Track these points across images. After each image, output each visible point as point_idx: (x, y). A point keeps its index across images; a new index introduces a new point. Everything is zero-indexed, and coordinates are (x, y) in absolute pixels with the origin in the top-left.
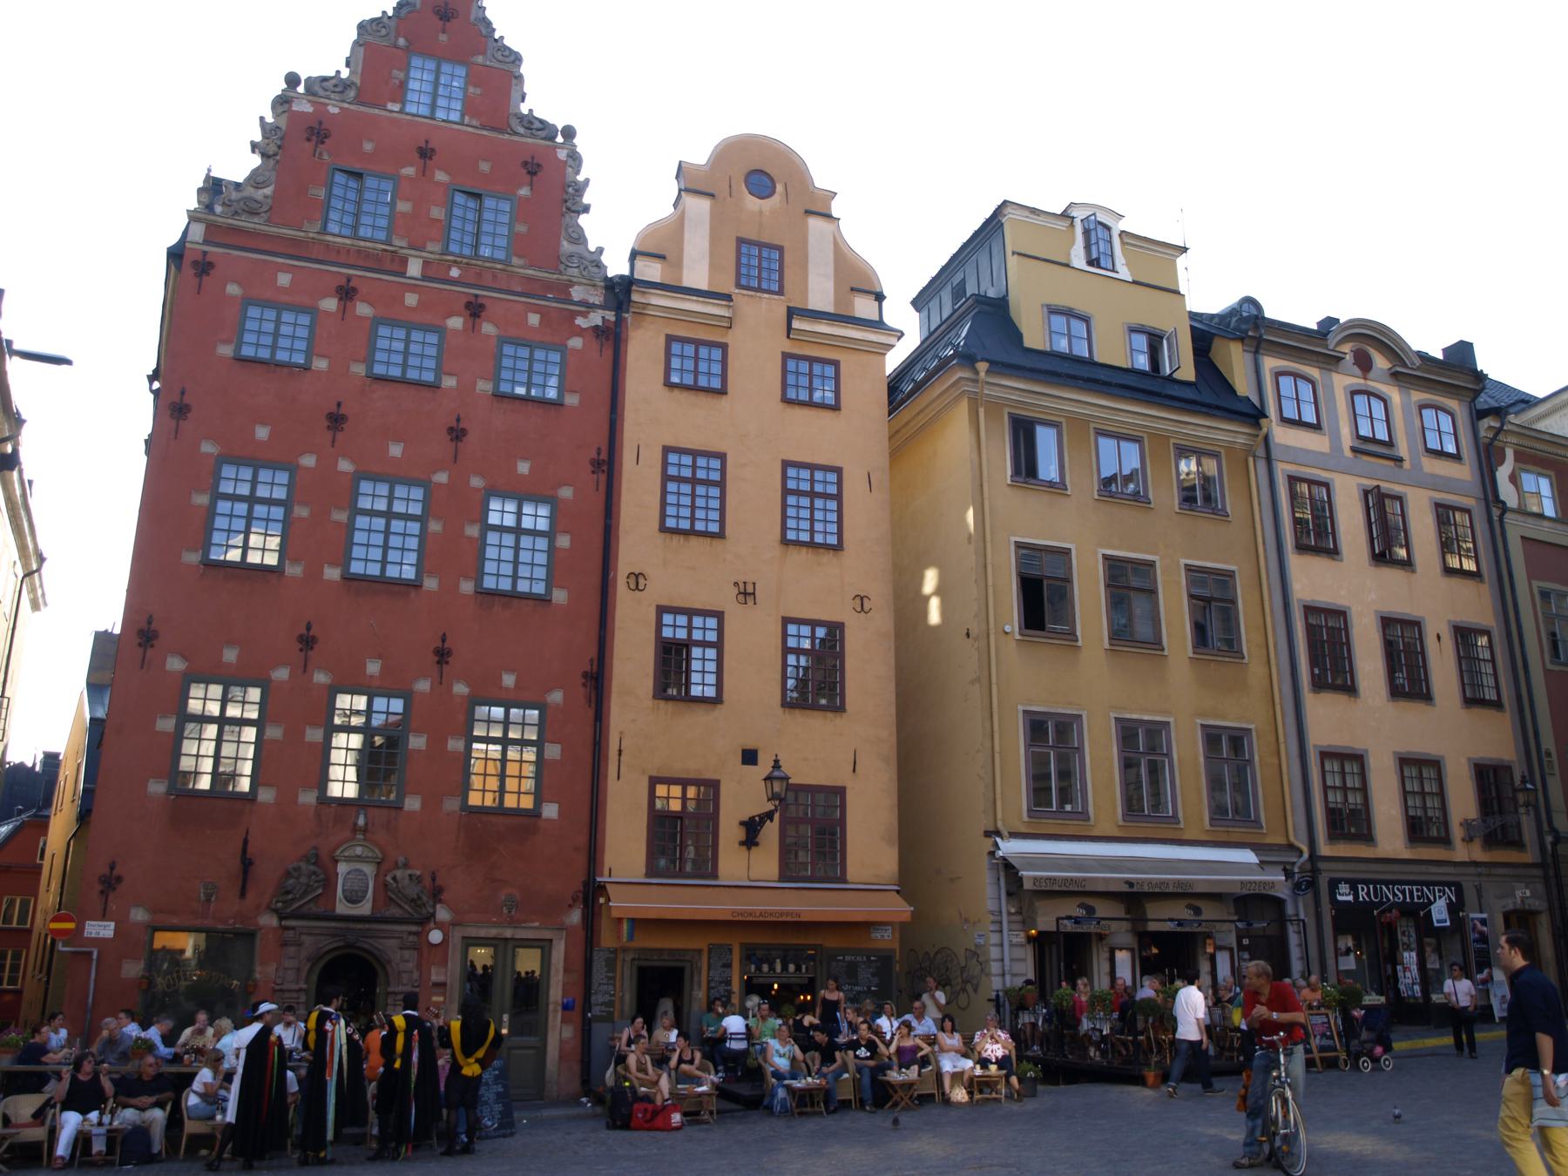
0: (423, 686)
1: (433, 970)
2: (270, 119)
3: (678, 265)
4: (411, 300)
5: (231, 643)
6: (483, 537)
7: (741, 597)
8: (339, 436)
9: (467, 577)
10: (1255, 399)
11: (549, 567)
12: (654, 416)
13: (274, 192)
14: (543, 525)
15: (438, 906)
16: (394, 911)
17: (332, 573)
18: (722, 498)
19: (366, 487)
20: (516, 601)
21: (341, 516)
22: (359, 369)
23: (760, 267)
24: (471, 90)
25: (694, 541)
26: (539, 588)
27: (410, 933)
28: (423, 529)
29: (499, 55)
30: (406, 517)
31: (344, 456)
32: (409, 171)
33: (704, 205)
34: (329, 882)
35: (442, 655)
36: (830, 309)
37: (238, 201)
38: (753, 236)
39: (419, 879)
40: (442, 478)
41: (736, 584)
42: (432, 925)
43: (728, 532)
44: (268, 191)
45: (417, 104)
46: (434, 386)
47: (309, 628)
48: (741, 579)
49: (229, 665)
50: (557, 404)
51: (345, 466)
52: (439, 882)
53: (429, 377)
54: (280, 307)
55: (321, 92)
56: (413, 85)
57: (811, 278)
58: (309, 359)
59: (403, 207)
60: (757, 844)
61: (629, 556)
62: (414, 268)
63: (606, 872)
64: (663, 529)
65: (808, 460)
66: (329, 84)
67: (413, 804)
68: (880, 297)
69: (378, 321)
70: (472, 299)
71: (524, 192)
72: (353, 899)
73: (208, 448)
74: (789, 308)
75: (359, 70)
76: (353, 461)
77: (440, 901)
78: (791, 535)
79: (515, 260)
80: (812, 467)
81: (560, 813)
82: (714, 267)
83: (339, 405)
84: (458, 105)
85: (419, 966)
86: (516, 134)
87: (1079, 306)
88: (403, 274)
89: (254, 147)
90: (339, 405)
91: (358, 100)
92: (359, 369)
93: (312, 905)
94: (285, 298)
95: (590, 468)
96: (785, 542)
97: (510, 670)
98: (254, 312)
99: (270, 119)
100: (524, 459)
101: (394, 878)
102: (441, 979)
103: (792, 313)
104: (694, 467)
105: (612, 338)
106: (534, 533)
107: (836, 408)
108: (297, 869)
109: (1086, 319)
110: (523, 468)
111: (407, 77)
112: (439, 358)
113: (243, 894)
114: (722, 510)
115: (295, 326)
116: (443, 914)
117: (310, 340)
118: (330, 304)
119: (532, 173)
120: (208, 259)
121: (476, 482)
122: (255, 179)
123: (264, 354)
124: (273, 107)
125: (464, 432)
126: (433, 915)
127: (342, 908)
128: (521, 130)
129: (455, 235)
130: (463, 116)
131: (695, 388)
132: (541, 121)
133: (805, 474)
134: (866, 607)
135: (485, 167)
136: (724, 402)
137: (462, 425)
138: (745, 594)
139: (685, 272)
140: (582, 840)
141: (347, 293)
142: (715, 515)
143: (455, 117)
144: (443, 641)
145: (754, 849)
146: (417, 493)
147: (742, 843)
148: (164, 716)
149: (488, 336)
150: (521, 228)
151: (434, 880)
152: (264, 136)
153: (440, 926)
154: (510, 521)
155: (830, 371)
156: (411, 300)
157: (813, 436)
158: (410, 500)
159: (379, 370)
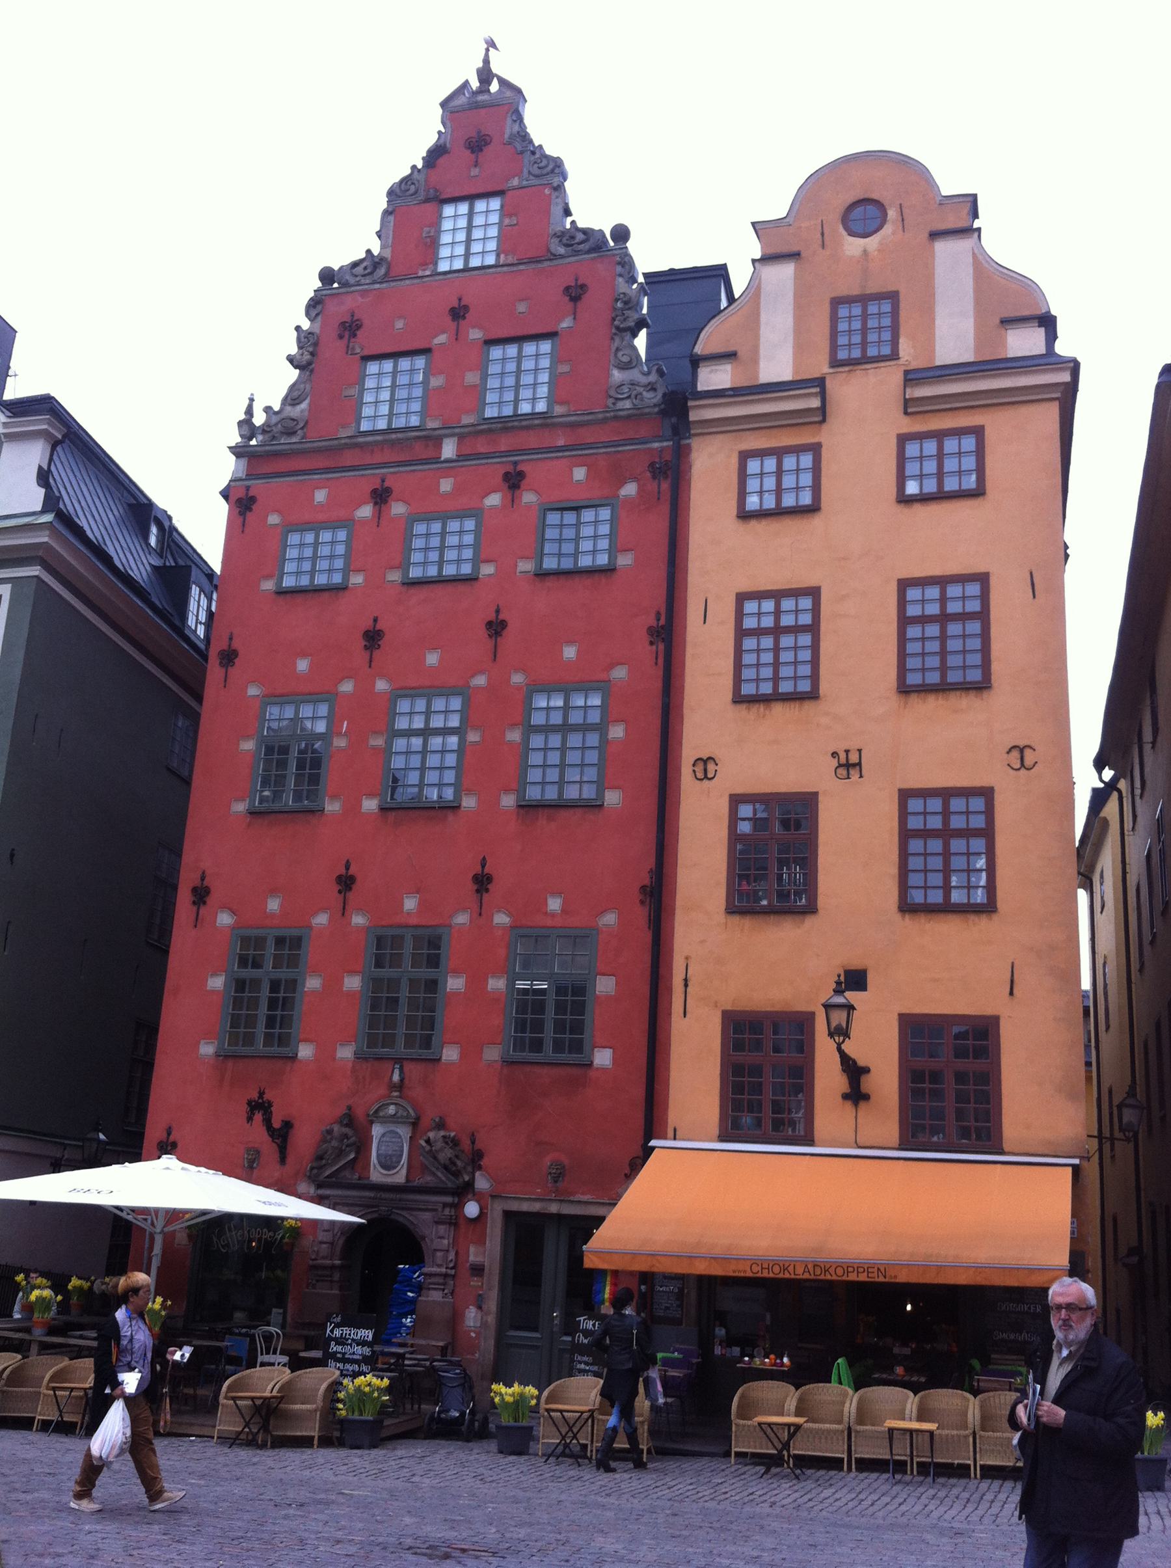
0: (462, 919)
1: (472, 1249)
2: (306, 325)
3: (755, 360)
5: (273, 891)
6: (526, 740)
7: (842, 772)
8: (376, 653)
9: (507, 790)
11: (601, 766)
13: (310, 405)
14: (594, 717)
15: (477, 1174)
16: (428, 1179)
17: (370, 805)
18: (815, 647)
19: (404, 706)
20: (564, 813)
21: (378, 741)
22: (395, 576)
23: (864, 330)
24: (507, 221)
25: (778, 708)
26: (589, 792)
27: (445, 1205)
28: (462, 741)
29: (535, 171)
30: (445, 732)
31: (382, 676)
32: (442, 339)
33: (785, 272)
34: (362, 1146)
35: (482, 882)
36: (968, 357)
37: (276, 424)
38: (856, 291)
39: (454, 1143)
40: (480, 681)
41: (834, 754)
42: (470, 1196)
43: (824, 687)
44: (304, 405)
45: (449, 259)
46: (471, 579)
47: (347, 868)
48: (840, 748)
49: (273, 915)
50: (609, 571)
51: (381, 685)
52: (479, 1145)
53: (466, 569)
54: (316, 526)
55: (352, 280)
56: (446, 238)
57: (937, 322)
58: (346, 577)
59: (436, 382)
60: (866, 1097)
61: (694, 741)
62: (449, 450)
63: (670, 1133)
64: (739, 699)
65: (937, 571)
66: (359, 270)
67: (450, 1054)
68: (1048, 323)
69: (413, 518)
70: (510, 468)
71: (566, 323)
72: (388, 1164)
73: (253, 691)
74: (906, 372)
75: (390, 241)
76: (390, 680)
77: (480, 1168)
78: (913, 679)
79: (559, 410)
80: (942, 581)
81: (614, 1059)
82: (800, 348)
83: (375, 620)
84: (492, 245)
85: (455, 1242)
86: (556, 257)
88: (436, 459)
89: (291, 359)
90: (375, 620)
91: (386, 278)
92: (395, 576)
93: (347, 1173)
94: (321, 517)
95: (646, 639)
96: (904, 690)
97: (556, 893)
98: (294, 539)
99: (306, 325)
100: (570, 642)
101: (428, 1141)
102: (479, 1259)
103: (912, 377)
104: (777, 613)
105: (671, 475)
106: (585, 728)
107: (978, 492)
108: (330, 1132)
110: (570, 652)
111: (439, 232)
112: (476, 546)
113: (283, 1160)
114: (815, 662)
115: (334, 541)
116: (482, 1183)
117: (347, 556)
118: (366, 512)
119: (575, 299)
120: (251, 494)
121: (517, 679)
122: (292, 398)
123: (305, 581)
124: (307, 314)
125: (503, 624)
126: (470, 1185)
127: (376, 1175)
128: (562, 250)
129: (491, 397)
130: (498, 256)
131: (780, 512)
132: (586, 232)
133: (933, 592)
134: (1028, 761)
135: (522, 307)
136: (817, 521)
137: (501, 617)
138: (848, 766)
139: (763, 364)
140: (638, 1092)
141: (381, 497)
142: (805, 670)
143: (490, 260)
144: (483, 867)
145: (862, 1104)
146: (456, 703)
147: (845, 1097)
148: (215, 974)
149: (529, 507)
150: (564, 368)
151: (473, 1143)
152: (300, 347)
153: (479, 1197)
155: (969, 443)
156: (446, 485)
157: (946, 540)
158: (448, 712)
159: (415, 573)
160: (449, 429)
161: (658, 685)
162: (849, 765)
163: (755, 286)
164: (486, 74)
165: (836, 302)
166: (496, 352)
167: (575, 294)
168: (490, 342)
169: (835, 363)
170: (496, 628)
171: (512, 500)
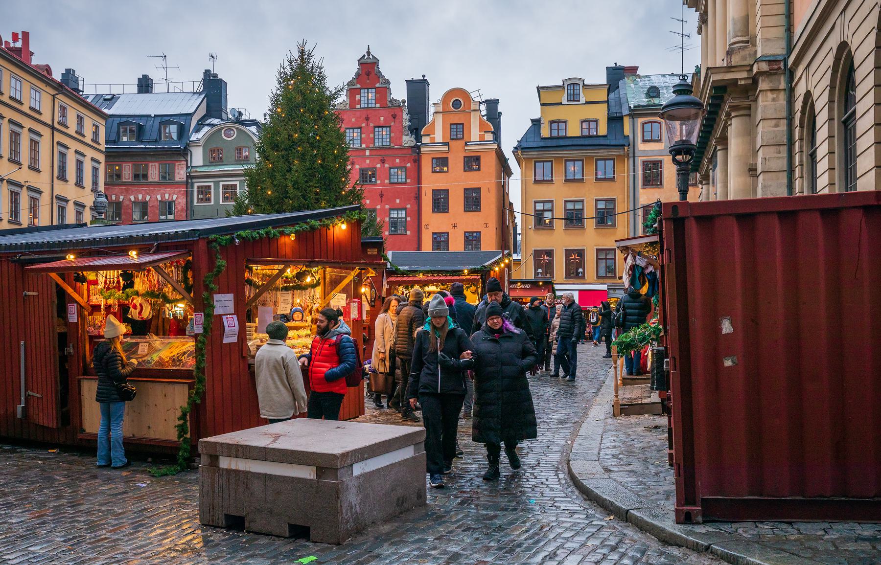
4: (368, 161)
14: (404, 215)
62: (368, 153)
103: (466, 144)
109: (565, 122)
110: (398, 201)
154: (396, 216)
157: (472, 180)
160: (367, 147)
163: (434, 121)
164: (369, 53)
165: (451, 125)
166: (377, 129)
168: (375, 127)
169: (451, 139)
170: (382, 196)
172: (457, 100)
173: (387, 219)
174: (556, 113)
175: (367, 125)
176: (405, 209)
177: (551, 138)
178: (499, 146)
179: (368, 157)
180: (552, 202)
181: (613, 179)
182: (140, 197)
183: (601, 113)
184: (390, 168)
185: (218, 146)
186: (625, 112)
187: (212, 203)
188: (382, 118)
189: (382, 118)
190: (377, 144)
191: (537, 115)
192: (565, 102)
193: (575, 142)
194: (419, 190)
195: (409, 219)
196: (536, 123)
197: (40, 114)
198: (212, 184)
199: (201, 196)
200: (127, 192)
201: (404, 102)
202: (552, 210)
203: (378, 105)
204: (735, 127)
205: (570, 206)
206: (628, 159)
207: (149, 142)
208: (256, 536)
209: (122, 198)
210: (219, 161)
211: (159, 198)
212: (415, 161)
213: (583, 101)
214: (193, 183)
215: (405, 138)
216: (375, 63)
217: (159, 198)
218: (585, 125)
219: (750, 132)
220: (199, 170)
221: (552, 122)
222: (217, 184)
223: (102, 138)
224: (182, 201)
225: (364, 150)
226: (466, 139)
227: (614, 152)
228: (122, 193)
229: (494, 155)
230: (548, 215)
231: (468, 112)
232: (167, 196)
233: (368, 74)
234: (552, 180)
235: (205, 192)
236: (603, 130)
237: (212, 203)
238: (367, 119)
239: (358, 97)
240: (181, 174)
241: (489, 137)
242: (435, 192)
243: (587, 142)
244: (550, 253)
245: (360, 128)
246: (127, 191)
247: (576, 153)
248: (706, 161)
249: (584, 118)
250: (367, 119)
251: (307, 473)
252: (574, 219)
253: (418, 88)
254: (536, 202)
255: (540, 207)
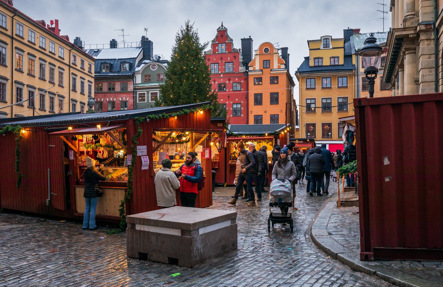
4: (222, 80)
10: (356, 65)
12: (253, 90)
14: (240, 107)
24: (227, 47)
32: (220, 62)
62: (222, 76)
87: (320, 56)
103: (271, 70)
109: (322, 58)
110: (237, 100)
154: (236, 107)
157: (274, 88)
160: (222, 73)
161: (246, 103)
162: (265, 112)
164: (222, 26)
166: (226, 64)
167: (235, 57)
168: (225, 63)
169: (264, 68)
170: (229, 97)
171: (229, 82)
172: (267, 48)
173: (231, 109)
174: (317, 54)
175: (222, 62)
176: (240, 103)
177: (315, 67)
178: (288, 71)
179: (222, 78)
180: (315, 99)
181: (347, 87)
182: (111, 99)
183: (340, 53)
184: (233, 83)
185: (149, 73)
186: (353, 52)
187: (146, 102)
188: (229, 58)
189: (229, 58)
190: (226, 71)
191: (308, 55)
192: (322, 48)
193: (327, 68)
194: (248, 94)
195: (242, 108)
196: (307, 59)
197: (64, 59)
198: (146, 92)
199: (140, 98)
200: (105, 97)
201: (240, 50)
202: (315, 103)
203: (227, 52)
204: (408, 59)
205: (324, 101)
206: (355, 77)
207: (115, 72)
208: (153, 263)
209: (102, 100)
210: (149, 81)
211: (120, 99)
212: (245, 80)
213: (331, 47)
214: (136, 92)
215: (240, 68)
216: (225, 30)
217: (120, 99)
218: (332, 60)
219: (415, 62)
220: (139, 85)
221: (315, 58)
222: (148, 92)
223: (93, 71)
224: (131, 101)
225: (220, 74)
226: (271, 68)
227: (347, 73)
228: (102, 97)
229: (285, 76)
230: (313, 106)
231: (272, 54)
232: (124, 98)
233: (222, 36)
234: (315, 88)
235: (142, 96)
236: (341, 62)
237: (146, 102)
238: (221, 59)
239: (217, 48)
240: (131, 88)
241: (283, 66)
242: (256, 95)
243: (333, 68)
244: (314, 125)
245: (218, 63)
246: (105, 96)
247: (328, 74)
248: (393, 77)
249: (331, 56)
250: (221, 59)
251: (176, 233)
252: (327, 108)
253: (247, 43)
254: (307, 99)
255: (309, 102)
